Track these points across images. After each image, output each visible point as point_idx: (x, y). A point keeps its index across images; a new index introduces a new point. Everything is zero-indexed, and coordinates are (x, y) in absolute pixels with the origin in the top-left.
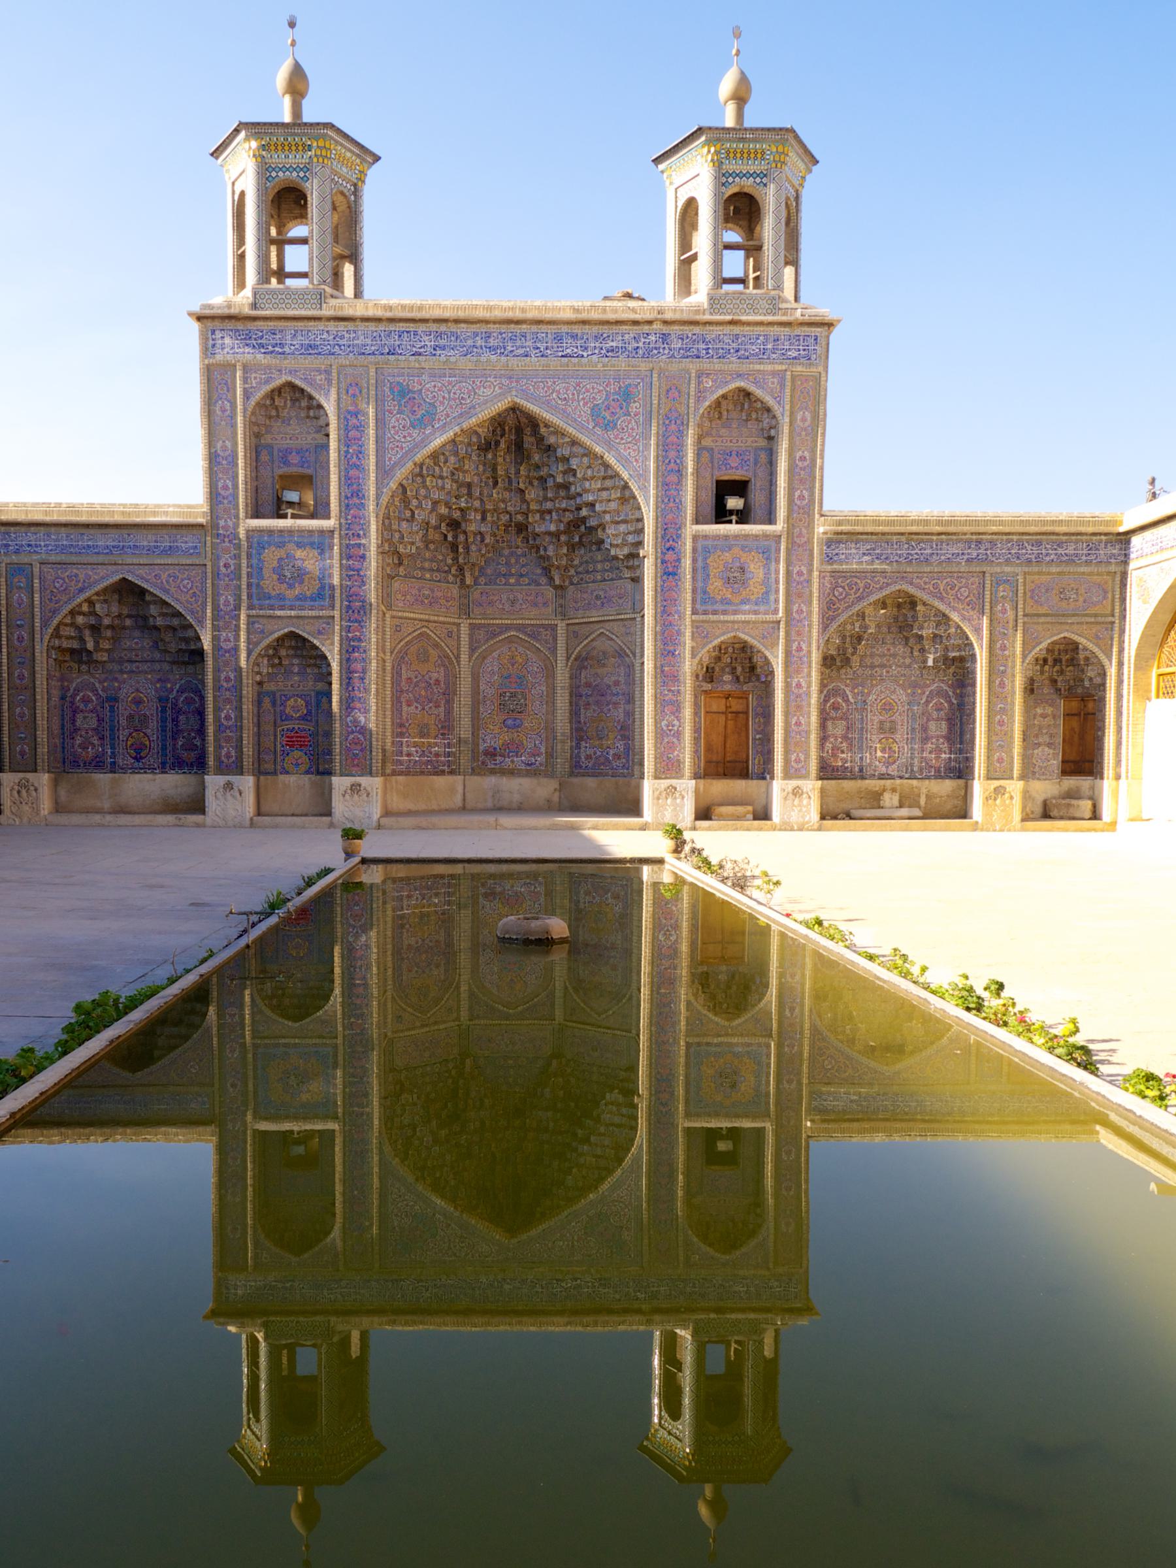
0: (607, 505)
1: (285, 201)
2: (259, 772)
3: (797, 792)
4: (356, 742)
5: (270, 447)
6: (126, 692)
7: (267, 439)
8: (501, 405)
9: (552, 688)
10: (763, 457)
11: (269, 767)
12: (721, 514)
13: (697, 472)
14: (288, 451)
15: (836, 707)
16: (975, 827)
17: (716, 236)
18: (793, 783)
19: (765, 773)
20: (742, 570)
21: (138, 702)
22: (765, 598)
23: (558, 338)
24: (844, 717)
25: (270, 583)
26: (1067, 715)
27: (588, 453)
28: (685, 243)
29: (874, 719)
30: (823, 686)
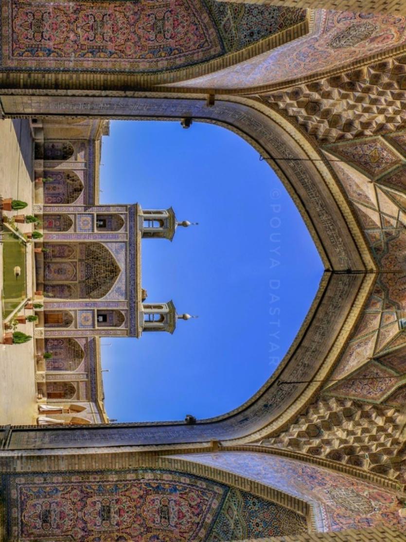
0: (101, 291)
1: (162, 222)
2: (44, 215)
3: (42, 333)
4: (50, 237)
5: (112, 218)
6: (61, 186)
7: (113, 218)
8: (120, 268)
9: (63, 280)
10: (111, 325)
11: (45, 217)
12: (98, 316)
13: (107, 310)
14: (111, 222)
15: (60, 342)
16: (35, 372)
17: (157, 313)
18: (43, 332)
19: (45, 327)
20: (88, 320)
21: (59, 188)
22: (82, 325)
23: (134, 280)
24: (58, 345)
25: (84, 218)
26: (60, 393)
27: (112, 286)
28: (155, 307)
29: (58, 351)
30: (65, 338)
